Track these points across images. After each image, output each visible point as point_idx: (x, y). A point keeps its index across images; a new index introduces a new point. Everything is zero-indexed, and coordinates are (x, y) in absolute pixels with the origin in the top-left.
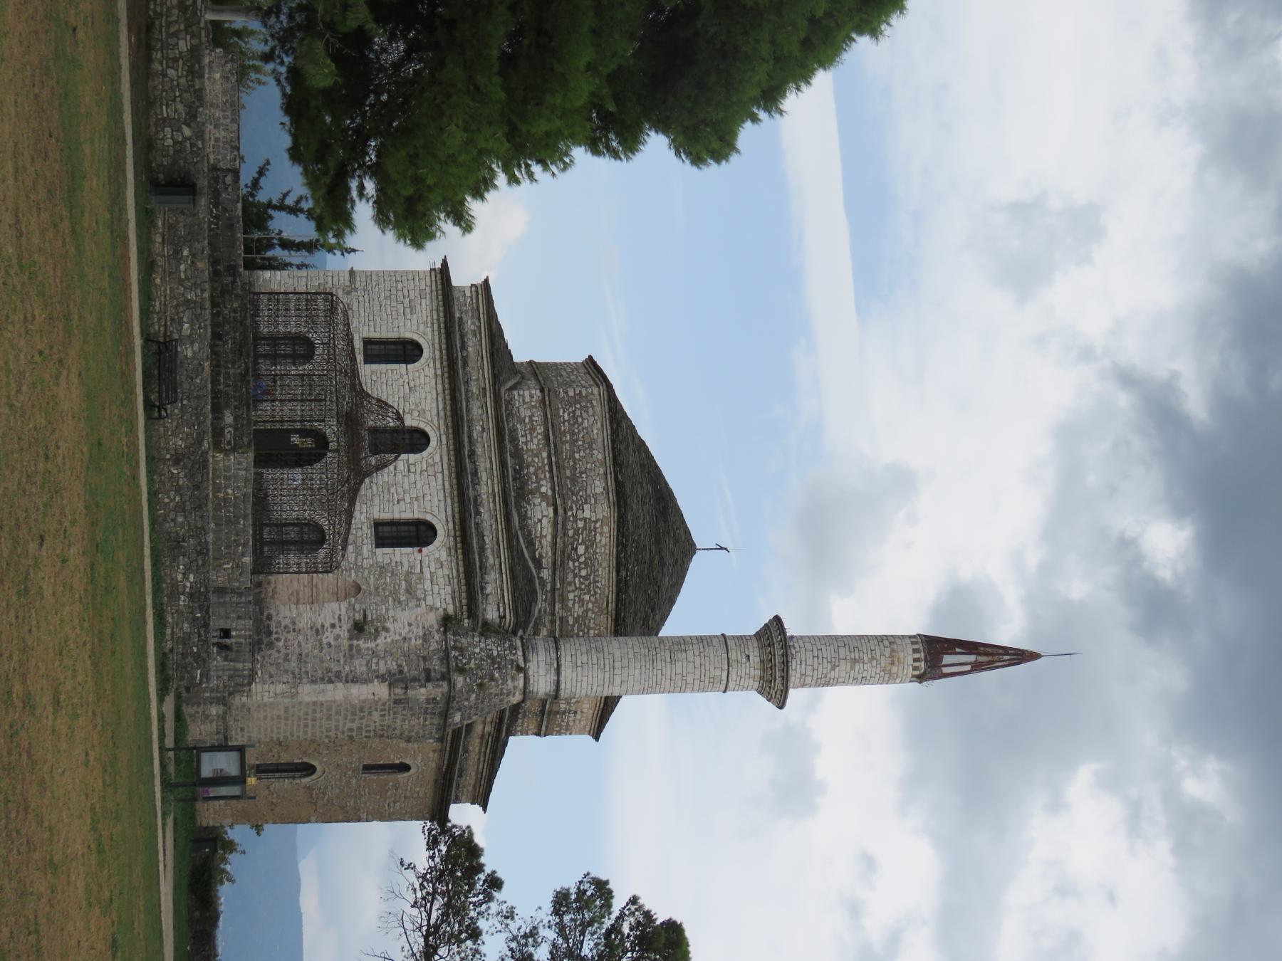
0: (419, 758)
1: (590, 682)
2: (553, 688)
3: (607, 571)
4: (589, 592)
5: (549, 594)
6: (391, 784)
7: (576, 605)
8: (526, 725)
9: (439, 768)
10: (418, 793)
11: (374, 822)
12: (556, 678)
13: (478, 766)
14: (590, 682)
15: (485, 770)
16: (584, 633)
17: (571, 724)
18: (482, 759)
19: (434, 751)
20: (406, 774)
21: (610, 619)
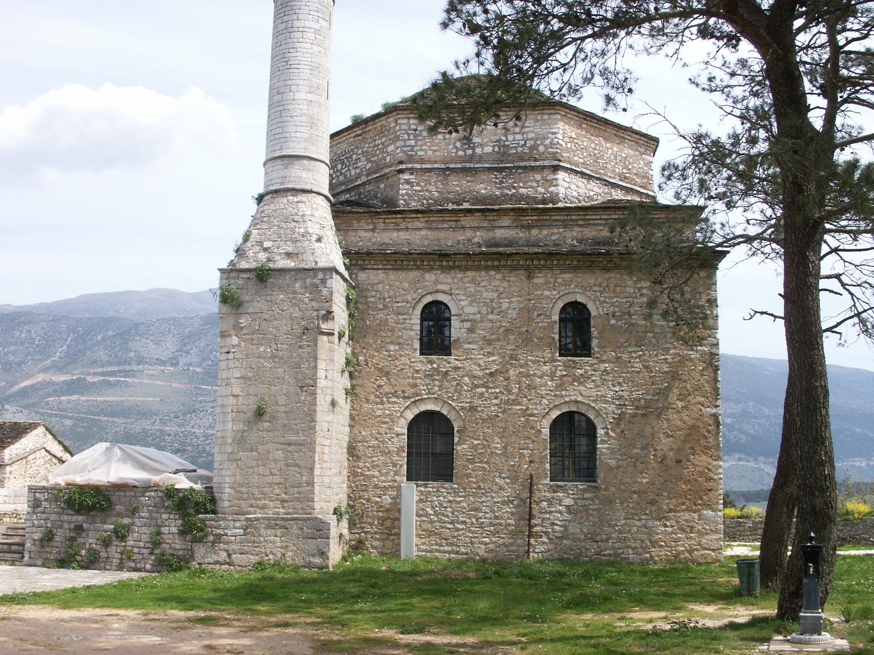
0: (547, 293)
1: (276, 126)
2: (279, 162)
3: (339, 146)
4: (351, 156)
5: (353, 194)
6: (613, 322)
7: (359, 164)
8: (535, 184)
9: (575, 269)
10: (640, 289)
11: (718, 336)
12: (270, 163)
13: (601, 225)
14: (276, 126)
15: (603, 217)
16: (378, 149)
17: (531, 135)
18: (581, 223)
19: (529, 278)
20: (591, 306)
21: (368, 129)
